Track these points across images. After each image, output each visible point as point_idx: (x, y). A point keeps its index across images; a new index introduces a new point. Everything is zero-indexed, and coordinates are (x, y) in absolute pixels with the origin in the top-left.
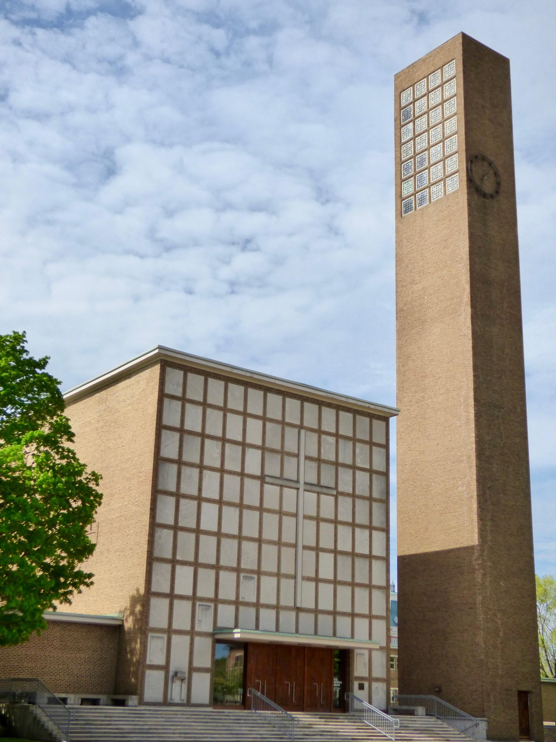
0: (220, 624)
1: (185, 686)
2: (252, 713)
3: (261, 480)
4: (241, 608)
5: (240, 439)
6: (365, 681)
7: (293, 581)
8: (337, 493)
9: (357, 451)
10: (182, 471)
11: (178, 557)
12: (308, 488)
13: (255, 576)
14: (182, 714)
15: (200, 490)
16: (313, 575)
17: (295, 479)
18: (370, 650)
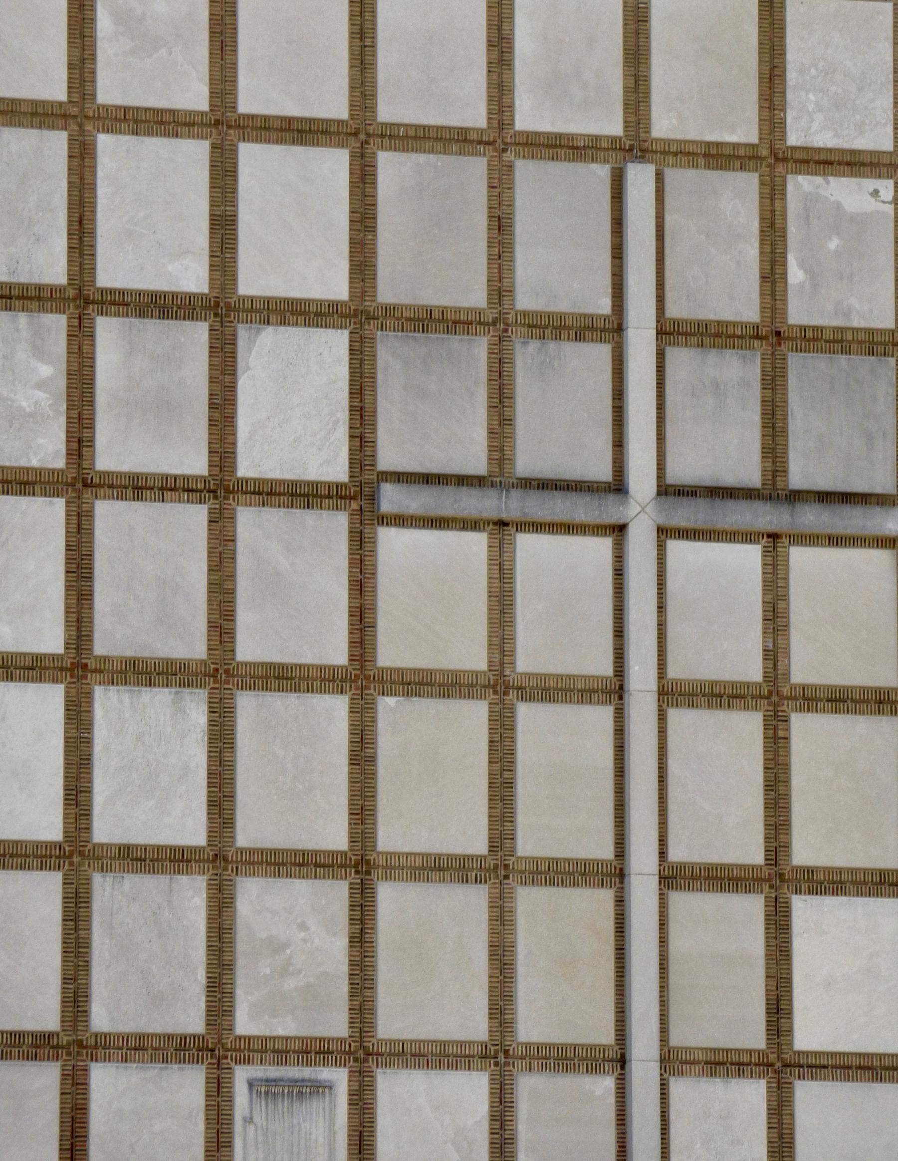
3: (355, 505)
7: (606, 1084)
17: (603, 472)
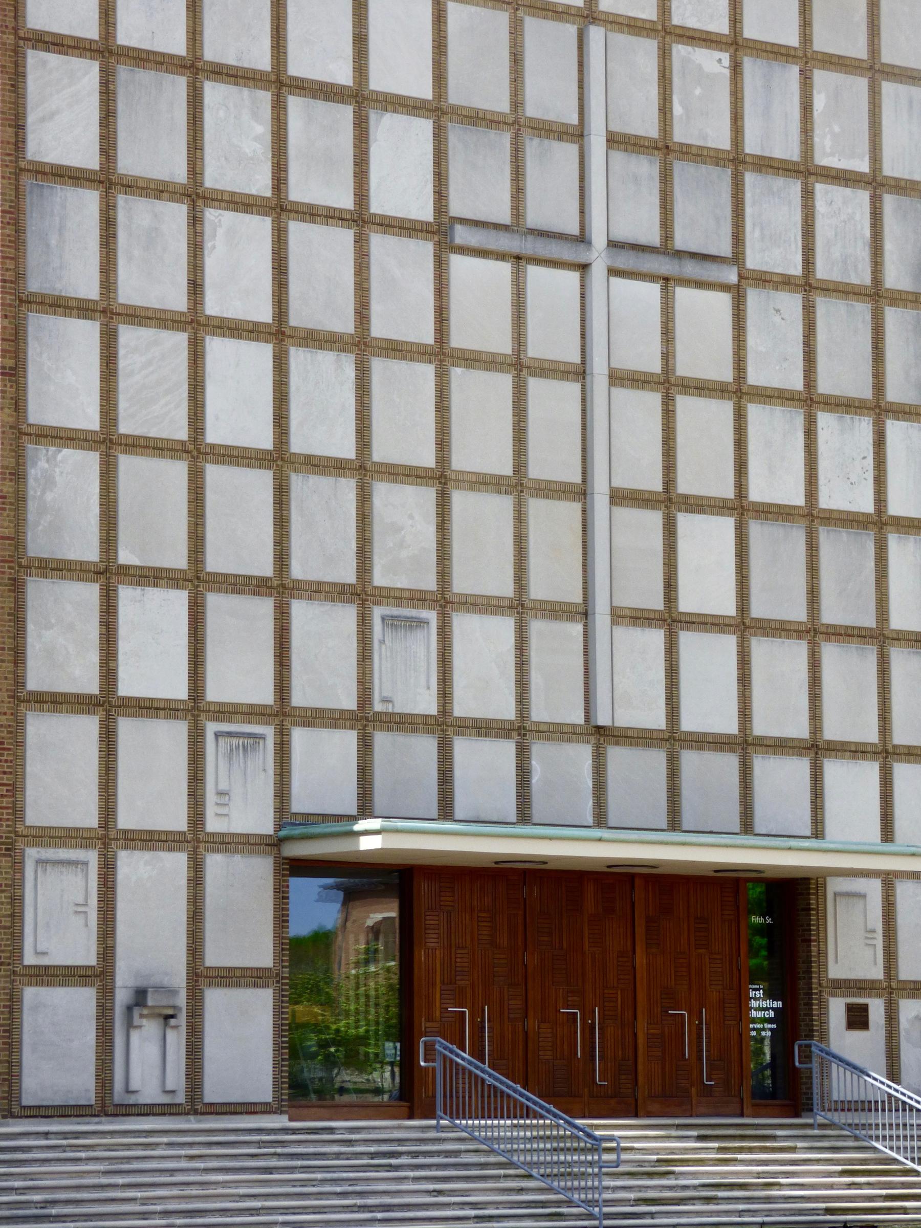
0: (300, 804)
1: (177, 1040)
2: (437, 1128)
4: (382, 740)
5: (343, 75)
6: (870, 996)
7: (577, 629)
8: (740, 276)
9: (819, 102)
10: (121, 217)
11: (126, 556)
12: (625, 261)
13: (432, 616)
14: (170, 1145)
15: (196, 287)
16: (657, 603)
17: (575, 230)
18: (889, 879)
